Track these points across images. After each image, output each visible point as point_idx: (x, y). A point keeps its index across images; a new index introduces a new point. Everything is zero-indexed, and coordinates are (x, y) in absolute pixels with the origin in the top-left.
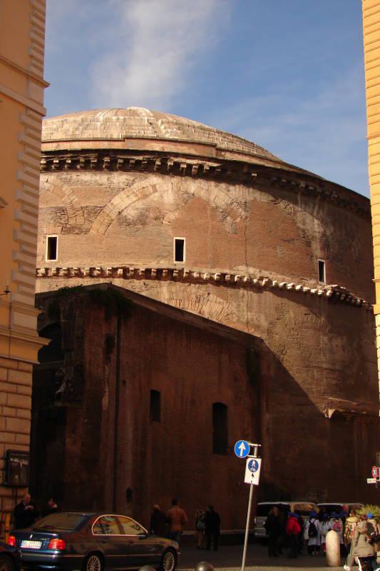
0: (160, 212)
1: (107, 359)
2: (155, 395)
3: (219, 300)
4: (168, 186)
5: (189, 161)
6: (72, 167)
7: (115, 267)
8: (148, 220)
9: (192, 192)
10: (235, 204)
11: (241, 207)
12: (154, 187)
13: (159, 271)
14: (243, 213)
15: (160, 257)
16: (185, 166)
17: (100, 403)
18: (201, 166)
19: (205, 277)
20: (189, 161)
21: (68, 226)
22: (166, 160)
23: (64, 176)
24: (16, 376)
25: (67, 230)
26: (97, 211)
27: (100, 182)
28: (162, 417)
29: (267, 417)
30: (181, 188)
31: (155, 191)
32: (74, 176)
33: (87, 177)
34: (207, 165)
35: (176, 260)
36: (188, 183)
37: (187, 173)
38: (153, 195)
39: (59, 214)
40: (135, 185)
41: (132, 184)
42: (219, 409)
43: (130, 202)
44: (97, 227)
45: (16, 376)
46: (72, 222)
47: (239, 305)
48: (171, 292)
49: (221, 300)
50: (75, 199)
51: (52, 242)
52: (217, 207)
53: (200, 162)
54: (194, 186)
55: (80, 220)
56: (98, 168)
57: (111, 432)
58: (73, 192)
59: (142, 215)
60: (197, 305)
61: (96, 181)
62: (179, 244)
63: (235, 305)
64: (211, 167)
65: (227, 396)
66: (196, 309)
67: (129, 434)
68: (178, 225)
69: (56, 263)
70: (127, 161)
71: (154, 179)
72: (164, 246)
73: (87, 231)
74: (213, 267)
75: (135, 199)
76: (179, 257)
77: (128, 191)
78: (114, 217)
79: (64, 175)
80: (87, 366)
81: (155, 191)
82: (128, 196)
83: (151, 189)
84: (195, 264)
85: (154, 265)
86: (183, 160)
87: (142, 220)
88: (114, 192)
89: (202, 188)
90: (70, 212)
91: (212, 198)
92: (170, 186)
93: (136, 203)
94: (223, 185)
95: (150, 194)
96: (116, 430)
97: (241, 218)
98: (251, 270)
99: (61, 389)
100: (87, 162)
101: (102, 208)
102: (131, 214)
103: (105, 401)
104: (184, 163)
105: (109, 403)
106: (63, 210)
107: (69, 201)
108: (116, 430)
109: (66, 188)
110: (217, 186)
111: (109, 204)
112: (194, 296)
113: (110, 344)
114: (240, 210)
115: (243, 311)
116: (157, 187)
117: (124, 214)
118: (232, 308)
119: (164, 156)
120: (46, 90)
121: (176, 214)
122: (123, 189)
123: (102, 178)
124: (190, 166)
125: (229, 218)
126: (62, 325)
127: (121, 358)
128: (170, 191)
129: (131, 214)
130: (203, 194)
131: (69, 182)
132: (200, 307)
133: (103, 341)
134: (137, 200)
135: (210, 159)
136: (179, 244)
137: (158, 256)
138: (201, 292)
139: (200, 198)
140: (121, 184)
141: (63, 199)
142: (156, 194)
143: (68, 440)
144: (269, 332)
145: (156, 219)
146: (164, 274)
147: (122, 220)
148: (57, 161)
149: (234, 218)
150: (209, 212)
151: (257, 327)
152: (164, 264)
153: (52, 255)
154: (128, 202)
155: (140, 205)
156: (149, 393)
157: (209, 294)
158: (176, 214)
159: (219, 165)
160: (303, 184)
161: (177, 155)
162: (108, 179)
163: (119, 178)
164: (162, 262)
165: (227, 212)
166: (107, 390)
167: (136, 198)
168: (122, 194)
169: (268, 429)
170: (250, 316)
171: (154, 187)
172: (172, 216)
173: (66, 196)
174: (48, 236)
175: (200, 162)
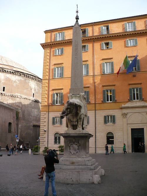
3: (11, 100)
18: (10, 72)
20: (8, 70)
29: (20, 126)
42: (10, 124)
53: (10, 70)
54: (9, 76)
62: (4, 88)
64: (12, 72)
65: (12, 121)
68: (4, 84)
76: (4, 90)
84: (7, 92)
91: (12, 78)
98: (19, 94)
110: (13, 76)
125: (15, 83)
130: (10, 77)
136: (4, 88)
138: (8, 98)
150: (11, 81)
151: (19, 107)
160: (31, 77)
161: (5, 68)
165: (15, 82)
169: (20, 128)
172: (3, 81)
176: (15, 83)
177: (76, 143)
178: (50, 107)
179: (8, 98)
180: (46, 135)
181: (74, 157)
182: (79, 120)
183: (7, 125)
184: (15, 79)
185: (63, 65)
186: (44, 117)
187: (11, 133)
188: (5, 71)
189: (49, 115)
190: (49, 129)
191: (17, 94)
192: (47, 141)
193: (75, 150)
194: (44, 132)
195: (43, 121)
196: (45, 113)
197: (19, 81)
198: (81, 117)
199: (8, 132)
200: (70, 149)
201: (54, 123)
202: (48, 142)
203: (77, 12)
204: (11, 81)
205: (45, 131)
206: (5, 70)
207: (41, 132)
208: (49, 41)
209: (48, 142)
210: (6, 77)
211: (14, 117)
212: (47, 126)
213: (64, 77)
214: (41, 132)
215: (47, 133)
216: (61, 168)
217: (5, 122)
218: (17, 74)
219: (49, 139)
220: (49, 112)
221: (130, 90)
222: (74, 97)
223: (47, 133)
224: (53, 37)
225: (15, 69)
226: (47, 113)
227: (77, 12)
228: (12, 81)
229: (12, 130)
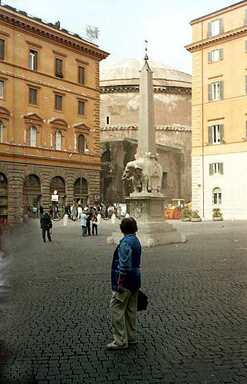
19: (161, 128)
24: (95, 174)
25: (113, 114)
26: (122, 107)
32: (114, 94)
33: (119, 95)
34: (162, 88)
44: (123, 113)
45: (95, 174)
50: (115, 103)
51: (108, 118)
56: (122, 92)
70: (133, 89)
73: (119, 114)
74: (164, 124)
79: (111, 94)
90: (113, 107)
91: (164, 100)
94: (168, 95)
98: (178, 125)
99: (111, 171)
100: (119, 89)
101: (125, 106)
106: (111, 107)
109: (112, 99)
120: (102, 63)
123: (124, 95)
129: (135, 107)
131: (112, 97)
144: (185, 147)
151: (180, 145)
153: (108, 123)
165: (170, 105)
170: (177, 141)
191: (175, 125)
194: (198, 187)
195: (196, 170)
196: (198, 157)
197: (176, 102)
201: (211, 173)
205: (199, 185)
213: (225, 98)
215: (202, 187)
223: (202, 187)
225: (170, 84)
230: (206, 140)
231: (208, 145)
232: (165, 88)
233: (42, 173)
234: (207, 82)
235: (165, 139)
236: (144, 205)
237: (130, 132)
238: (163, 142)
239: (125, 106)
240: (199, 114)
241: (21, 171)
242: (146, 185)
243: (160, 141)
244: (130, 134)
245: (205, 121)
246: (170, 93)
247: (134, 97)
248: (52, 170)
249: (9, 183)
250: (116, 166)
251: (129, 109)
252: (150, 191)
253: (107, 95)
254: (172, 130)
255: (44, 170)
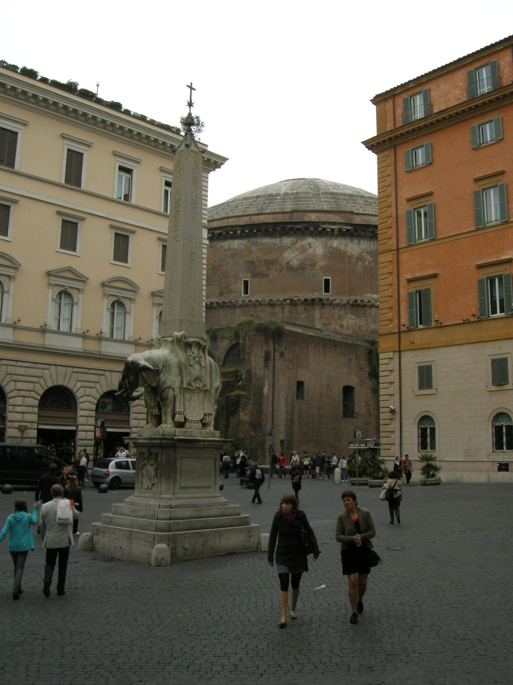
0: (314, 261)
1: (266, 365)
2: (300, 384)
3: (353, 317)
4: (319, 244)
5: (332, 227)
6: (255, 235)
7: (285, 298)
8: (306, 267)
9: (335, 246)
10: (364, 253)
11: (368, 254)
12: (310, 244)
13: (313, 300)
14: (370, 258)
15: (313, 290)
16: (330, 230)
17: (262, 390)
18: (340, 230)
19: (345, 302)
20: (332, 227)
21: (255, 273)
22: (318, 226)
23: (252, 240)
25: (255, 275)
27: (275, 243)
28: (305, 397)
30: (328, 244)
31: (310, 247)
33: (266, 240)
34: (345, 228)
35: (325, 292)
36: (332, 240)
37: (332, 234)
38: (309, 250)
39: (249, 265)
40: (297, 244)
41: (296, 244)
42: (348, 391)
43: (294, 255)
46: (258, 270)
47: (367, 320)
48: (321, 313)
49: (355, 317)
50: (259, 255)
51: (246, 283)
52: (352, 255)
53: (339, 227)
54: (335, 243)
55: (263, 269)
57: (270, 409)
58: (258, 250)
59: (302, 263)
60: (339, 321)
61: (272, 243)
62: (327, 282)
63: (364, 319)
64: (348, 230)
65: (353, 381)
66: (338, 324)
67: (282, 410)
68: (326, 269)
69: (248, 297)
71: (310, 240)
72: (317, 283)
73: (268, 275)
75: (297, 253)
76: (327, 290)
77: (293, 248)
78: (284, 265)
79: (253, 240)
80: (253, 370)
81: (310, 247)
82: (293, 252)
83: (308, 246)
84: (337, 294)
85: (310, 296)
86: (328, 226)
87: (302, 267)
88: (283, 249)
89: (342, 244)
92: (320, 243)
93: (298, 256)
94: (356, 241)
95: (307, 250)
96: (273, 406)
97: (369, 262)
100: (267, 230)
101: (277, 261)
102: (295, 263)
103: (266, 390)
104: (329, 228)
105: (268, 390)
106: (252, 263)
107: (256, 257)
108: (273, 406)
109: (253, 248)
110: (352, 241)
111: (281, 257)
112: (336, 316)
113: (267, 357)
114: (368, 256)
115: (370, 323)
116: (312, 244)
117: (291, 263)
118: (363, 322)
119: (316, 224)
121: (325, 262)
122: (290, 247)
123: (276, 241)
124: (333, 230)
125: (360, 262)
126: (241, 344)
127: (276, 364)
128: (320, 247)
129: (295, 263)
130: (342, 247)
131: (255, 244)
132: (341, 322)
133: (263, 355)
134: (299, 254)
135: (346, 224)
136: (327, 282)
137: (313, 290)
139: (340, 251)
140: (289, 244)
141: (252, 255)
142: (311, 249)
143: (241, 414)
145: (311, 265)
146: (316, 302)
147: (289, 267)
148: (248, 231)
149: (364, 262)
150: (346, 259)
152: (316, 295)
153: (246, 292)
154: (293, 255)
155: (300, 257)
156: (296, 384)
157: (347, 313)
158: (325, 262)
159: (352, 228)
161: (324, 223)
162: (280, 241)
163: (287, 241)
164: (316, 294)
165: (360, 258)
166: (266, 383)
167: (298, 252)
168: (289, 251)
171: (310, 244)
172: (322, 263)
173: (254, 253)
174: (243, 280)
175: (339, 227)
176: (360, 262)
177: (151, 462)
178: (403, 335)
179: (342, 312)
180: (395, 425)
181: (147, 495)
182: (161, 404)
183: (338, 393)
184: (360, 251)
185: (433, 200)
186: (390, 367)
187: (352, 417)
188: (324, 229)
189: (403, 359)
190: (404, 404)
191: (369, 295)
192: (398, 442)
193: (150, 479)
194: (389, 415)
196: (390, 355)
198: (164, 395)
199: (342, 414)
200: (142, 476)
202: (401, 444)
203: (190, 104)
204: (346, 259)
205: (393, 412)
206: (323, 226)
207: (384, 416)
208: (390, 127)
209: (401, 444)
210: (332, 247)
211: (361, 369)
212: (397, 396)
214: (382, 416)
216: (111, 522)
217: (328, 386)
218: (363, 234)
219: (404, 434)
220: (400, 351)
221: (480, 282)
222: (162, 344)
224: (399, 111)
225: (358, 220)
226: (397, 355)
227: (190, 104)
228: (349, 257)
229: (356, 409)
230: (404, 319)
231: (409, 331)
232: (350, 228)
233: (79, 384)
234: (404, 208)
235: (352, 322)
236: (163, 458)
237: (287, 309)
238: (348, 328)
239: (277, 261)
240: (392, 268)
241: (36, 379)
242: (169, 410)
243: (342, 326)
244: (286, 314)
245: (403, 283)
246: (360, 237)
247: (293, 244)
248: (46, 372)
249: (10, 401)
250: (249, 372)
251: (284, 265)
252: (180, 425)
253: (245, 241)
254: (364, 306)
255: (81, 377)
